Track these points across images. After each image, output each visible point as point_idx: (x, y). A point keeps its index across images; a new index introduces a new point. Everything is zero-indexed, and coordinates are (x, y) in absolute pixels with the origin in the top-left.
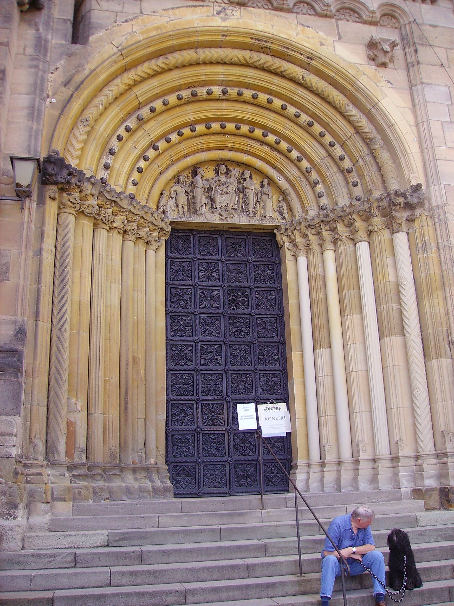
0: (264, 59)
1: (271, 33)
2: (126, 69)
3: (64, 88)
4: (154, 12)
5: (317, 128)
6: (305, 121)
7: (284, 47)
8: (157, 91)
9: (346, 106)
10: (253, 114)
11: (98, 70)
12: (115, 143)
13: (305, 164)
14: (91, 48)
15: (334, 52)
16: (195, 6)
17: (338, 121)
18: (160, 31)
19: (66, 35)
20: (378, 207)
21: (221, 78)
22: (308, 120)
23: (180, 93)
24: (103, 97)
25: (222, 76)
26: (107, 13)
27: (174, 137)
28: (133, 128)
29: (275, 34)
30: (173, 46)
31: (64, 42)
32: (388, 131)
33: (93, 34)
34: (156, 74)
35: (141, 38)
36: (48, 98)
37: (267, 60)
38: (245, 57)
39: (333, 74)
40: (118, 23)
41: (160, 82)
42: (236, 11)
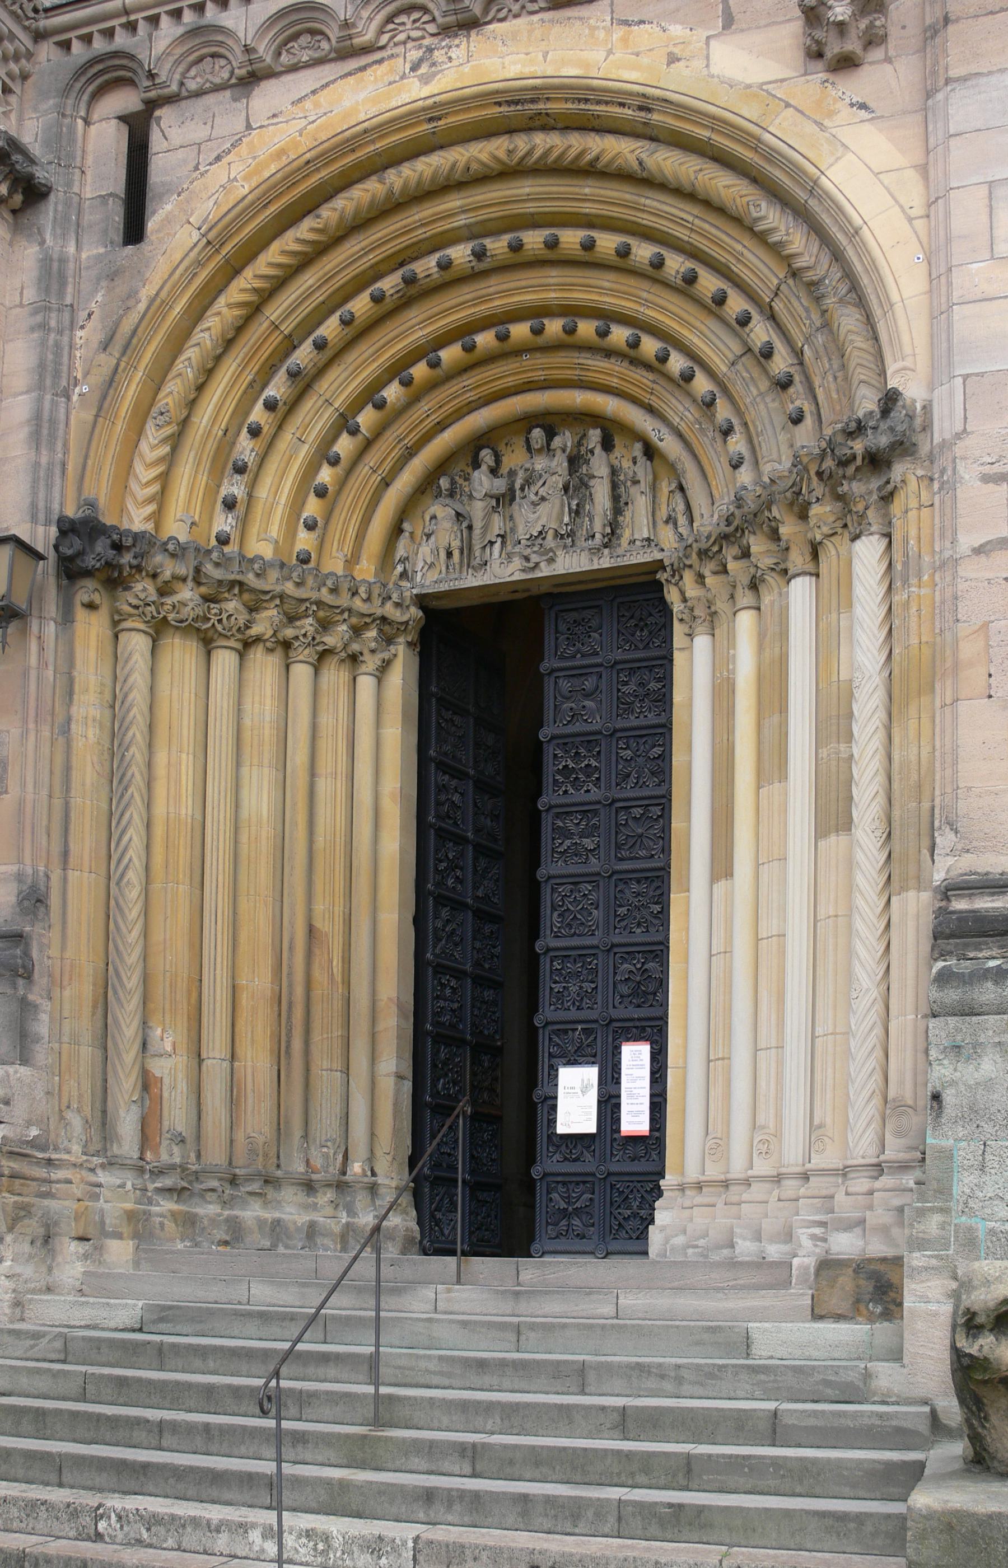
0: (542, 142)
1: (539, 74)
2: (233, 269)
3: (103, 356)
4: (274, 116)
5: (709, 283)
6: (678, 272)
7: (579, 100)
8: (319, 297)
9: (752, 208)
10: (563, 287)
11: (163, 294)
12: (245, 444)
13: (702, 384)
14: (150, 248)
15: (705, 72)
16: (363, 69)
17: (745, 252)
18: (284, 160)
19: (105, 231)
20: (819, 474)
21: (461, 220)
22: (682, 270)
23: (379, 285)
24: (192, 350)
25: (463, 217)
26: (181, 154)
27: (393, 392)
28: (284, 398)
29: (548, 74)
30: (321, 185)
31: (102, 250)
32: (850, 253)
33: (154, 213)
34: (304, 262)
35: (246, 191)
36: (76, 385)
37: (548, 146)
38: (497, 153)
39: (705, 134)
40: (202, 169)
41: (321, 273)
42: (457, 46)
